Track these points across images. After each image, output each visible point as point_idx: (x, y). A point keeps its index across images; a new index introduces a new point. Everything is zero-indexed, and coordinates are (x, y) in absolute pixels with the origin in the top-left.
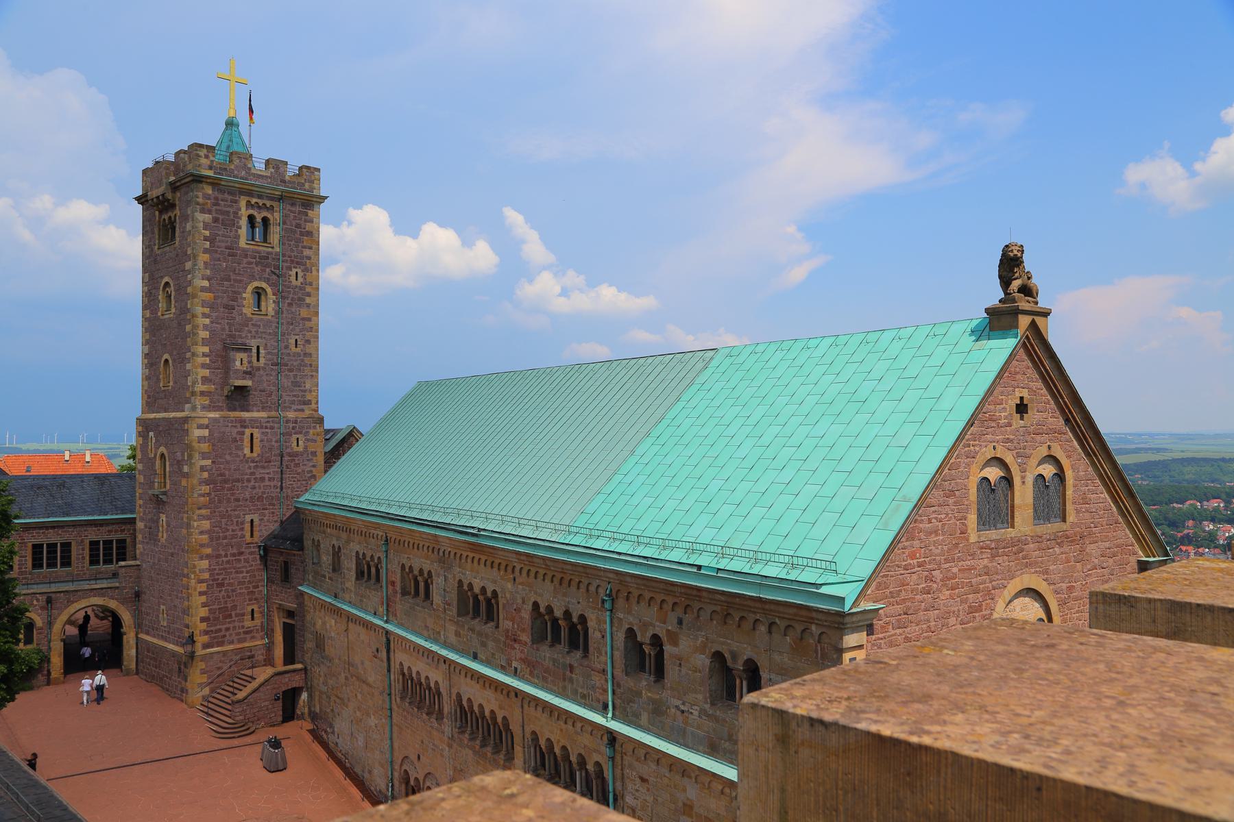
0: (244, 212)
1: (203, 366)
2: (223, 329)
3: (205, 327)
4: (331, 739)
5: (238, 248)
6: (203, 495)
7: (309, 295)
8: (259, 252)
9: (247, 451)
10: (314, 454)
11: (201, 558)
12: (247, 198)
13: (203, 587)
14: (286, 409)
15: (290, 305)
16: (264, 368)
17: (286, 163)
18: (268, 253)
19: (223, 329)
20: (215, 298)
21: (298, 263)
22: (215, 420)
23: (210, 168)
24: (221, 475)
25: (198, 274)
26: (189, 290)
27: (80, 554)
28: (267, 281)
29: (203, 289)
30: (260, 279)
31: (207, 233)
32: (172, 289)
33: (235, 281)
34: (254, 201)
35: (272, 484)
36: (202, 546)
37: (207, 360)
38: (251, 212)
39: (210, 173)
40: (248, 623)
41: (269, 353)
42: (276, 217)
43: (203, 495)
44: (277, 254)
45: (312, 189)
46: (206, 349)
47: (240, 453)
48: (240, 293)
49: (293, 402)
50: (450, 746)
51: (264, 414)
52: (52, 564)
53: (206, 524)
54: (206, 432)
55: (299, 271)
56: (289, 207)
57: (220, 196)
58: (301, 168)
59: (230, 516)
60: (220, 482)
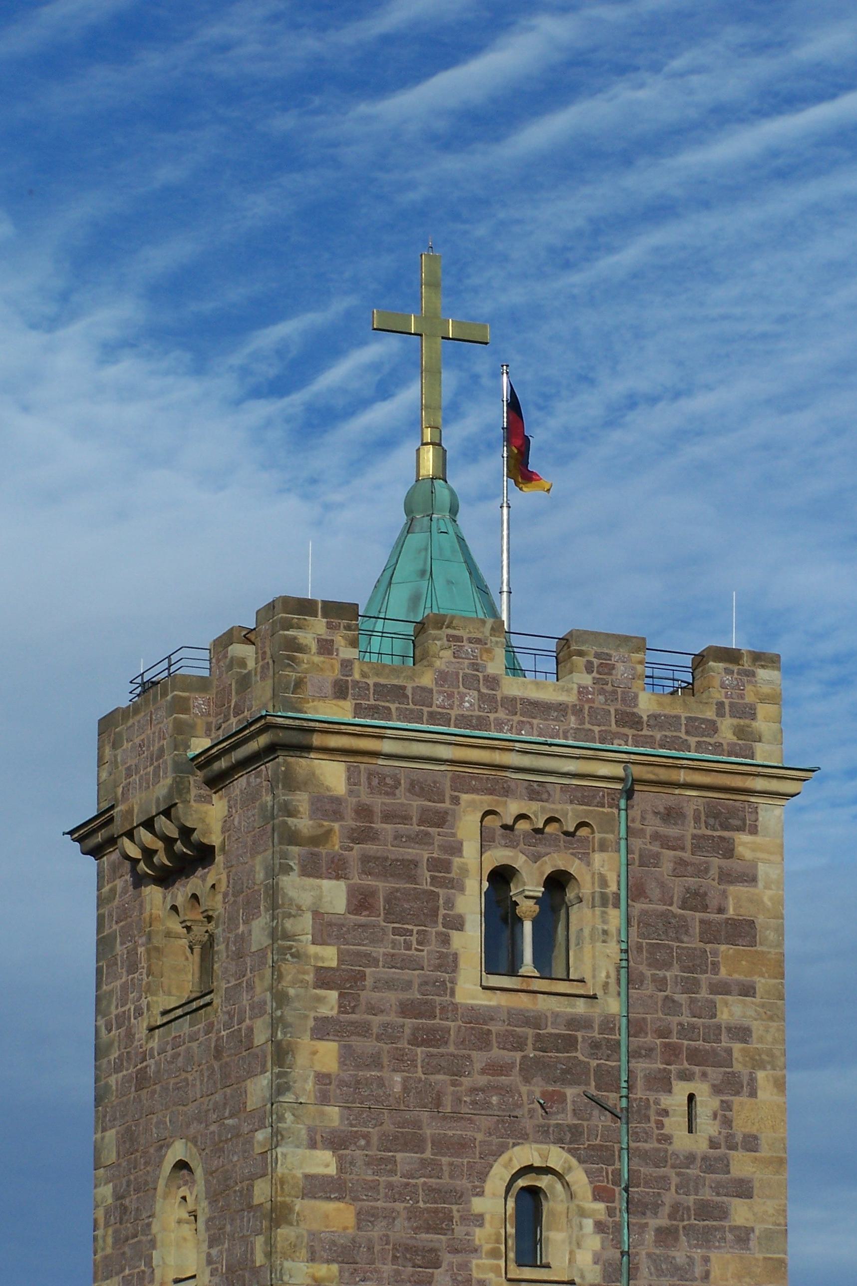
0: (473, 862)
7: (744, 1189)
8: (535, 1021)
12: (486, 801)
15: (666, 1235)
17: (640, 645)
18: (574, 1023)
20: (364, 1218)
21: (695, 1057)
23: (341, 691)
26: (261, 1192)
29: (317, 1187)
31: (329, 956)
33: (441, 1145)
34: (512, 808)
38: (499, 856)
39: (341, 711)
44: (608, 1024)
45: (748, 737)
48: (459, 1197)
55: (702, 1090)
56: (654, 825)
57: (378, 802)
58: (700, 660)
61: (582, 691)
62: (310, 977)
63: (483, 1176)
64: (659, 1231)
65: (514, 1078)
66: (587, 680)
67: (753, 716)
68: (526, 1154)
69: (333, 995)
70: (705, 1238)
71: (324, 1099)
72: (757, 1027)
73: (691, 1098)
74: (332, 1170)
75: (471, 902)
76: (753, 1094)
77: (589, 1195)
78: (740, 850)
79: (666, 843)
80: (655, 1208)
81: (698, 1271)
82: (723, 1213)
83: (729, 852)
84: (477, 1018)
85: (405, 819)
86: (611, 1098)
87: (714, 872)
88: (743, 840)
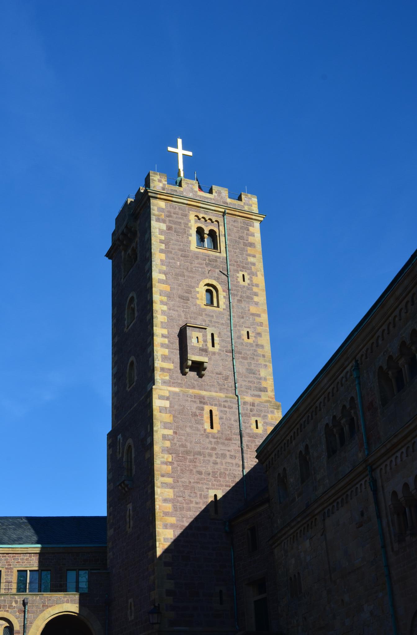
1: (162, 345)
2: (179, 316)
3: (163, 313)
5: (189, 251)
6: (166, 463)
7: (256, 294)
9: (207, 426)
11: (166, 526)
15: (239, 301)
16: (219, 354)
18: (216, 257)
19: (179, 316)
21: (243, 267)
22: (175, 393)
24: (183, 446)
28: (217, 279)
29: (160, 281)
30: (211, 277)
32: (135, 305)
33: (189, 277)
35: (234, 461)
36: (166, 514)
37: (166, 341)
38: (200, 225)
41: (223, 340)
42: (221, 231)
43: (166, 463)
46: (165, 332)
47: (200, 427)
48: (194, 287)
49: (249, 388)
51: (222, 395)
53: (169, 493)
54: (167, 404)
56: (232, 223)
57: (172, 210)
59: (193, 488)
61: (215, 196)
62: (158, 241)
63: (198, 284)
64: (238, 300)
65: (204, 266)
66: (216, 194)
67: (252, 206)
69: (164, 245)
70: (248, 302)
71: (162, 264)
72: (257, 264)
73: (243, 275)
74: (164, 278)
76: (257, 276)
77: (222, 290)
78: (250, 230)
79: (235, 227)
80: (237, 295)
81: (247, 309)
82: (252, 299)
83: (248, 230)
84: (195, 253)
85: (178, 214)
86: (226, 273)
87: (245, 233)
88: (251, 229)
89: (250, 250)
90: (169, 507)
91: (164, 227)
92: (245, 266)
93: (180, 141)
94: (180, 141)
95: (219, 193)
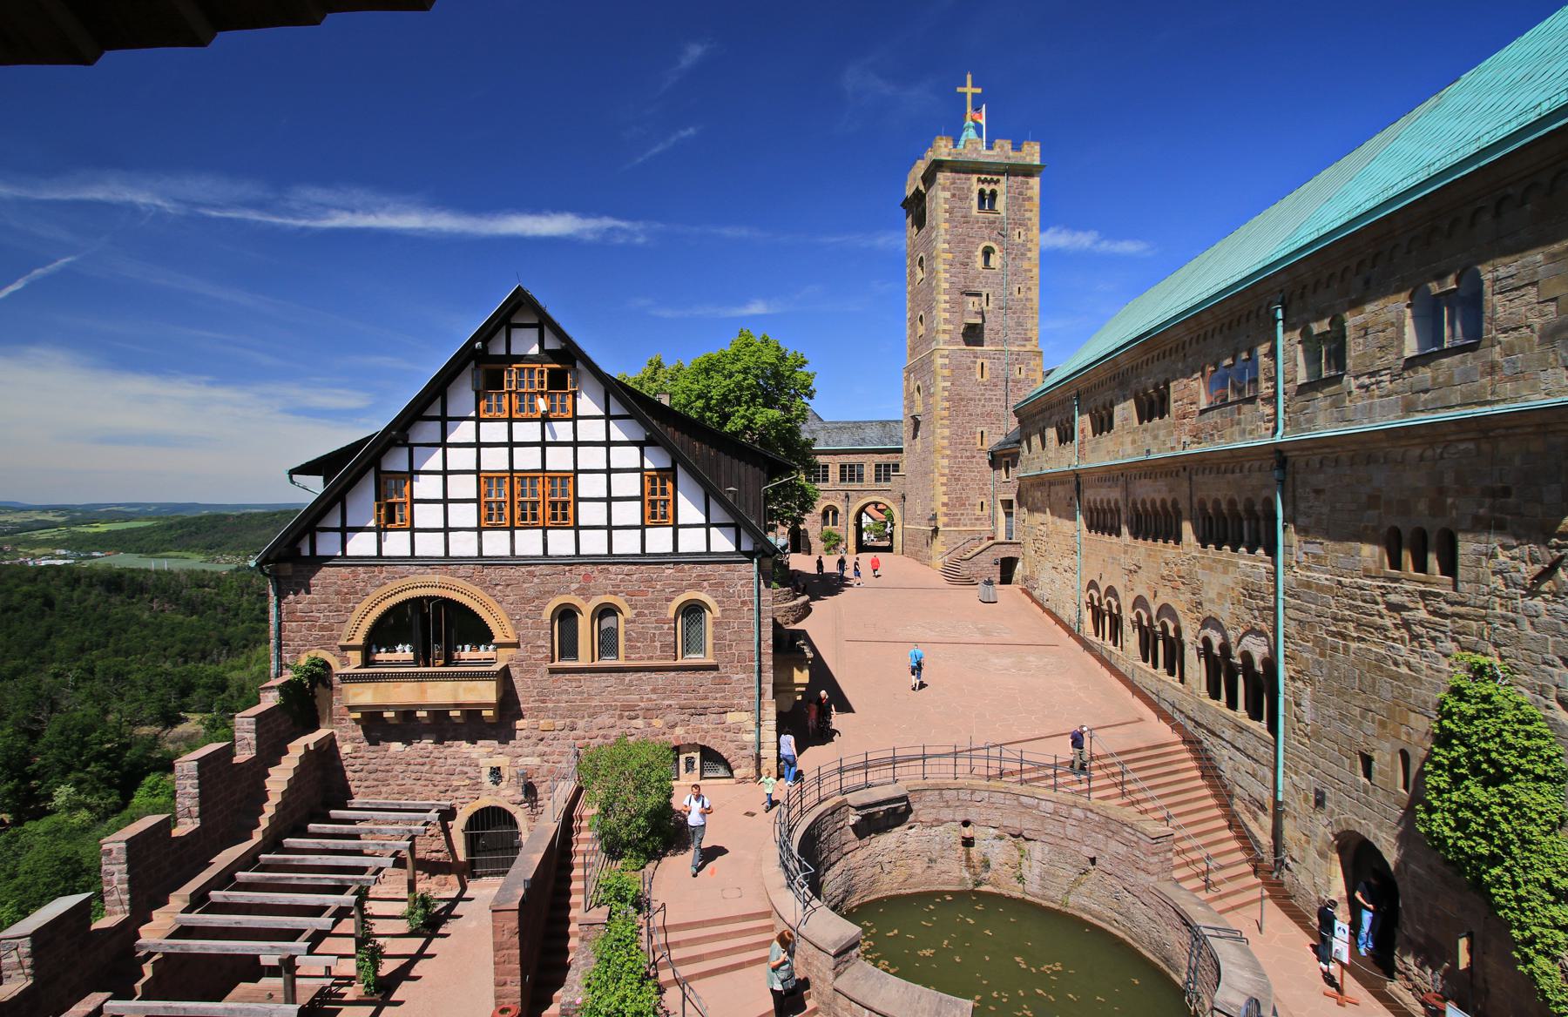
0: (976, 187)
4: (1036, 593)
9: (978, 376)
10: (1034, 381)
13: (944, 480)
14: (1010, 344)
25: (940, 239)
27: (869, 472)
28: (995, 241)
29: (944, 251)
40: (978, 512)
50: (1126, 552)
52: (852, 480)
53: (946, 432)
54: (946, 361)
60: (957, 401)
68: (987, 244)
75: (975, 196)
89: (1027, 205)
90: (945, 443)
91: (947, 195)
92: (1021, 223)
93: (969, 77)
94: (969, 77)
95: (1002, 147)
